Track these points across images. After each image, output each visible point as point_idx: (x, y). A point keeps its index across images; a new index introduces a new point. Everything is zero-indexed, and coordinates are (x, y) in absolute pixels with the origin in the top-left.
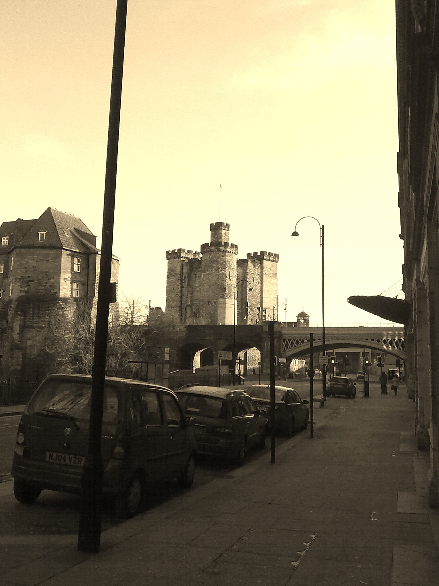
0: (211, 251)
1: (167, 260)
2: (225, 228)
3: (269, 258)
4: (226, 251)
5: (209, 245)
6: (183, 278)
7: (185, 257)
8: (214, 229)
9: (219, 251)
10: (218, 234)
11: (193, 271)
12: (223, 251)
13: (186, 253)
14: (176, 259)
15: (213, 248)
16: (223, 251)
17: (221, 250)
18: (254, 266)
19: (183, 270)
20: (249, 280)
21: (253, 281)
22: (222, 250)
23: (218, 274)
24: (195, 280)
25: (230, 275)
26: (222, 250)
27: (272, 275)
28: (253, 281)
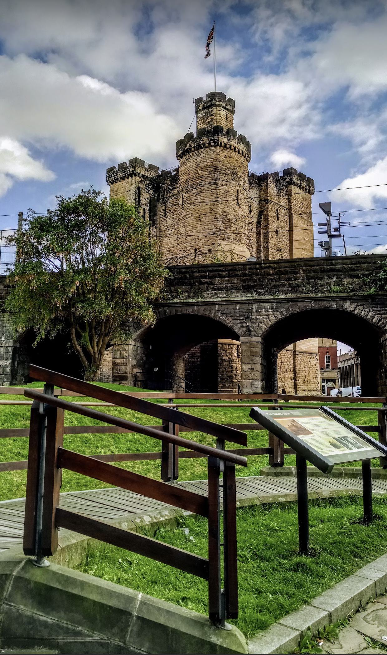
0: (199, 147)
1: (109, 186)
2: (226, 105)
3: (301, 183)
4: (230, 146)
5: (195, 136)
6: (142, 214)
7: (143, 176)
8: (204, 108)
9: (218, 145)
10: (212, 115)
11: (161, 197)
12: (226, 144)
13: (147, 170)
14: (126, 180)
15: (205, 140)
16: (226, 144)
17: (221, 143)
18: (279, 190)
19: (141, 199)
20: (272, 215)
21: (278, 219)
22: (223, 144)
23: (215, 191)
24: (165, 213)
25: (239, 198)
26: (223, 144)
27: (304, 216)
28: (278, 219)
